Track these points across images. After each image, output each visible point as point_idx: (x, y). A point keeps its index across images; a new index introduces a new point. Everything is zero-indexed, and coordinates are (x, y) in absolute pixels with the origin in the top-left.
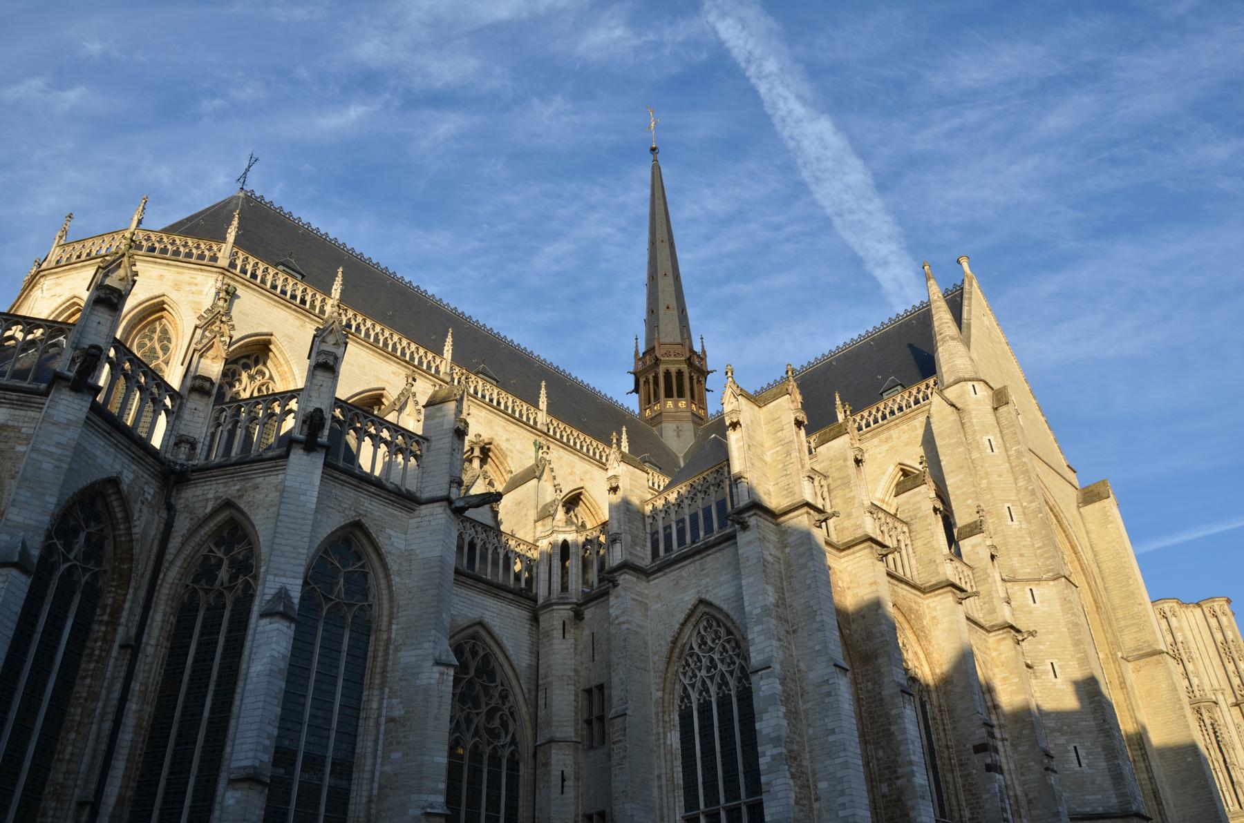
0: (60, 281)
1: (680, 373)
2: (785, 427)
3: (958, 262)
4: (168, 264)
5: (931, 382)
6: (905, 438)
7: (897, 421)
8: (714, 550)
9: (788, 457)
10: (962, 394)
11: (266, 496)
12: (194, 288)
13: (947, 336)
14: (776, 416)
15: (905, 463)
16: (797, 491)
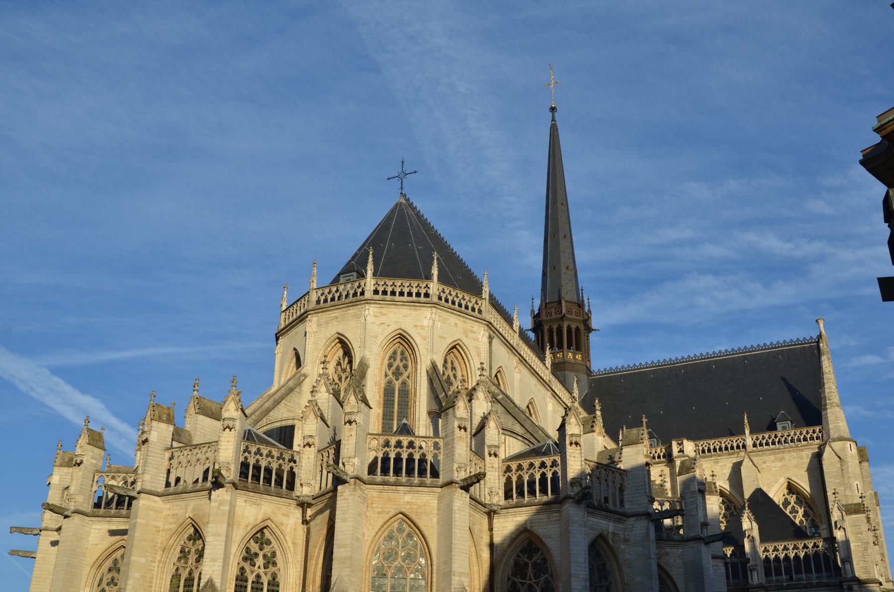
0: (384, 311)
1: (577, 329)
2: (863, 533)
3: (817, 321)
4: (459, 315)
5: (817, 429)
6: (794, 462)
7: (791, 449)
8: (815, 589)
9: (866, 551)
10: (844, 449)
11: (675, 561)
12: (474, 335)
13: (834, 403)
14: (857, 524)
15: (793, 479)
16: (872, 572)
